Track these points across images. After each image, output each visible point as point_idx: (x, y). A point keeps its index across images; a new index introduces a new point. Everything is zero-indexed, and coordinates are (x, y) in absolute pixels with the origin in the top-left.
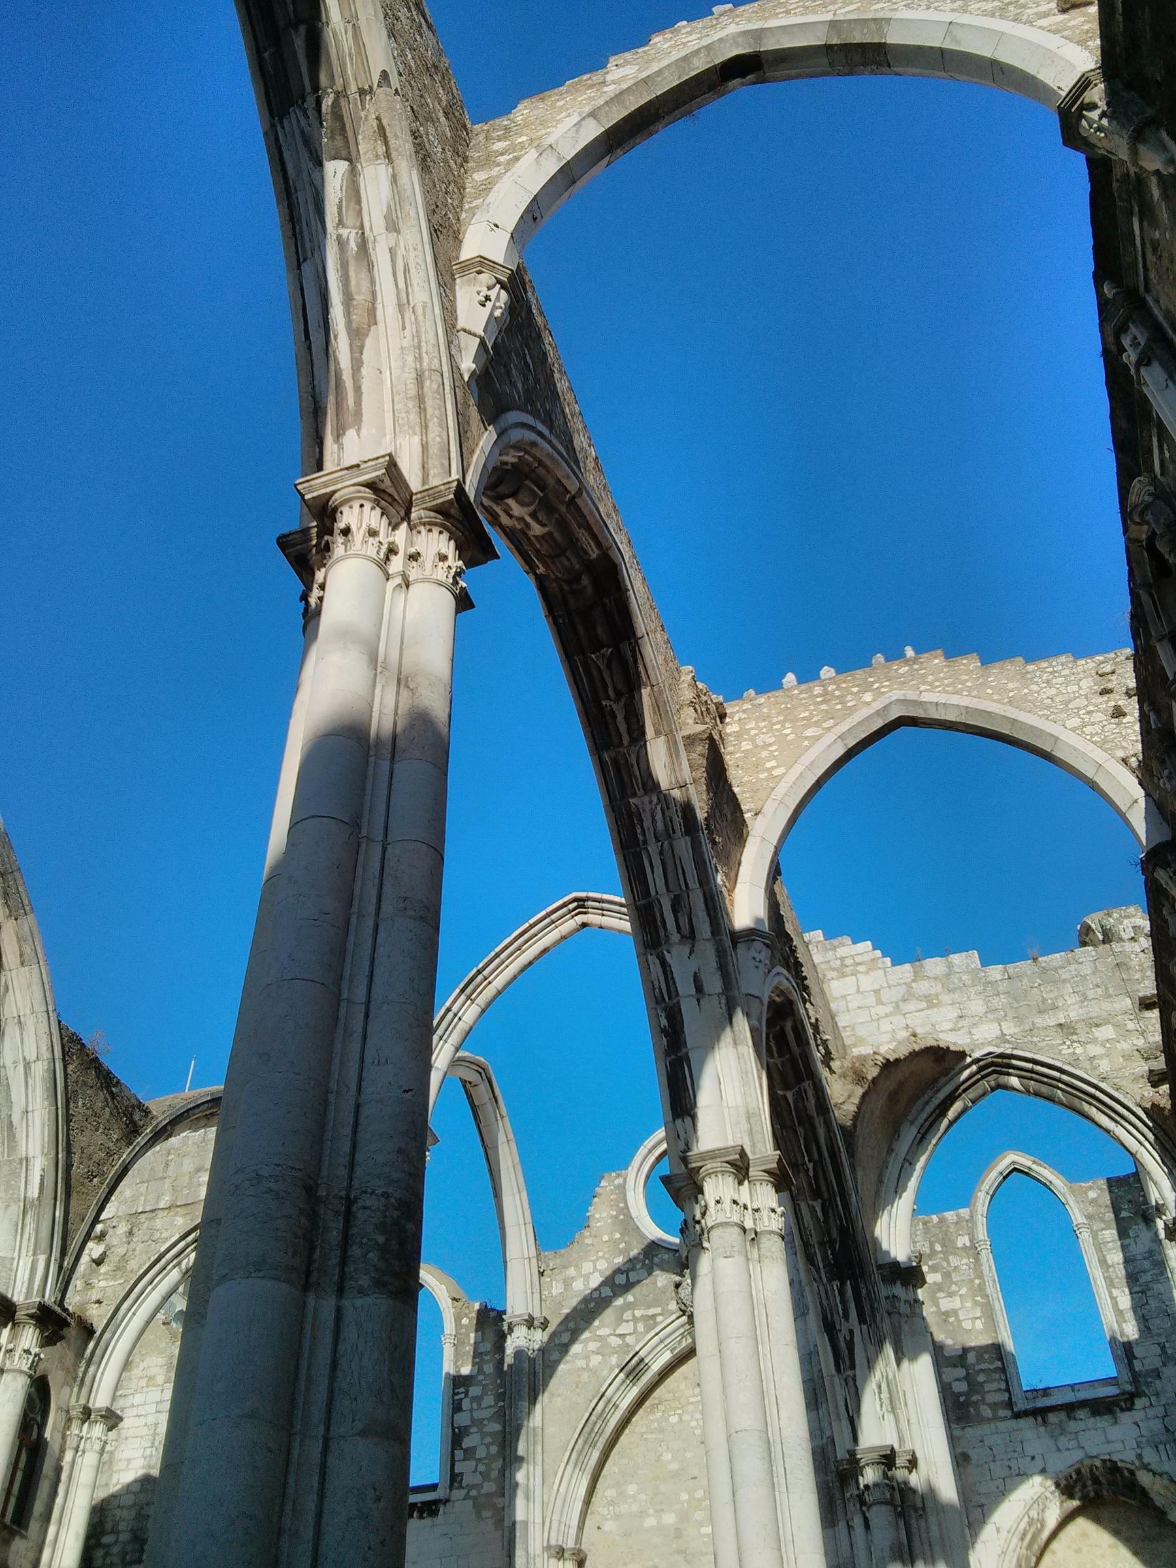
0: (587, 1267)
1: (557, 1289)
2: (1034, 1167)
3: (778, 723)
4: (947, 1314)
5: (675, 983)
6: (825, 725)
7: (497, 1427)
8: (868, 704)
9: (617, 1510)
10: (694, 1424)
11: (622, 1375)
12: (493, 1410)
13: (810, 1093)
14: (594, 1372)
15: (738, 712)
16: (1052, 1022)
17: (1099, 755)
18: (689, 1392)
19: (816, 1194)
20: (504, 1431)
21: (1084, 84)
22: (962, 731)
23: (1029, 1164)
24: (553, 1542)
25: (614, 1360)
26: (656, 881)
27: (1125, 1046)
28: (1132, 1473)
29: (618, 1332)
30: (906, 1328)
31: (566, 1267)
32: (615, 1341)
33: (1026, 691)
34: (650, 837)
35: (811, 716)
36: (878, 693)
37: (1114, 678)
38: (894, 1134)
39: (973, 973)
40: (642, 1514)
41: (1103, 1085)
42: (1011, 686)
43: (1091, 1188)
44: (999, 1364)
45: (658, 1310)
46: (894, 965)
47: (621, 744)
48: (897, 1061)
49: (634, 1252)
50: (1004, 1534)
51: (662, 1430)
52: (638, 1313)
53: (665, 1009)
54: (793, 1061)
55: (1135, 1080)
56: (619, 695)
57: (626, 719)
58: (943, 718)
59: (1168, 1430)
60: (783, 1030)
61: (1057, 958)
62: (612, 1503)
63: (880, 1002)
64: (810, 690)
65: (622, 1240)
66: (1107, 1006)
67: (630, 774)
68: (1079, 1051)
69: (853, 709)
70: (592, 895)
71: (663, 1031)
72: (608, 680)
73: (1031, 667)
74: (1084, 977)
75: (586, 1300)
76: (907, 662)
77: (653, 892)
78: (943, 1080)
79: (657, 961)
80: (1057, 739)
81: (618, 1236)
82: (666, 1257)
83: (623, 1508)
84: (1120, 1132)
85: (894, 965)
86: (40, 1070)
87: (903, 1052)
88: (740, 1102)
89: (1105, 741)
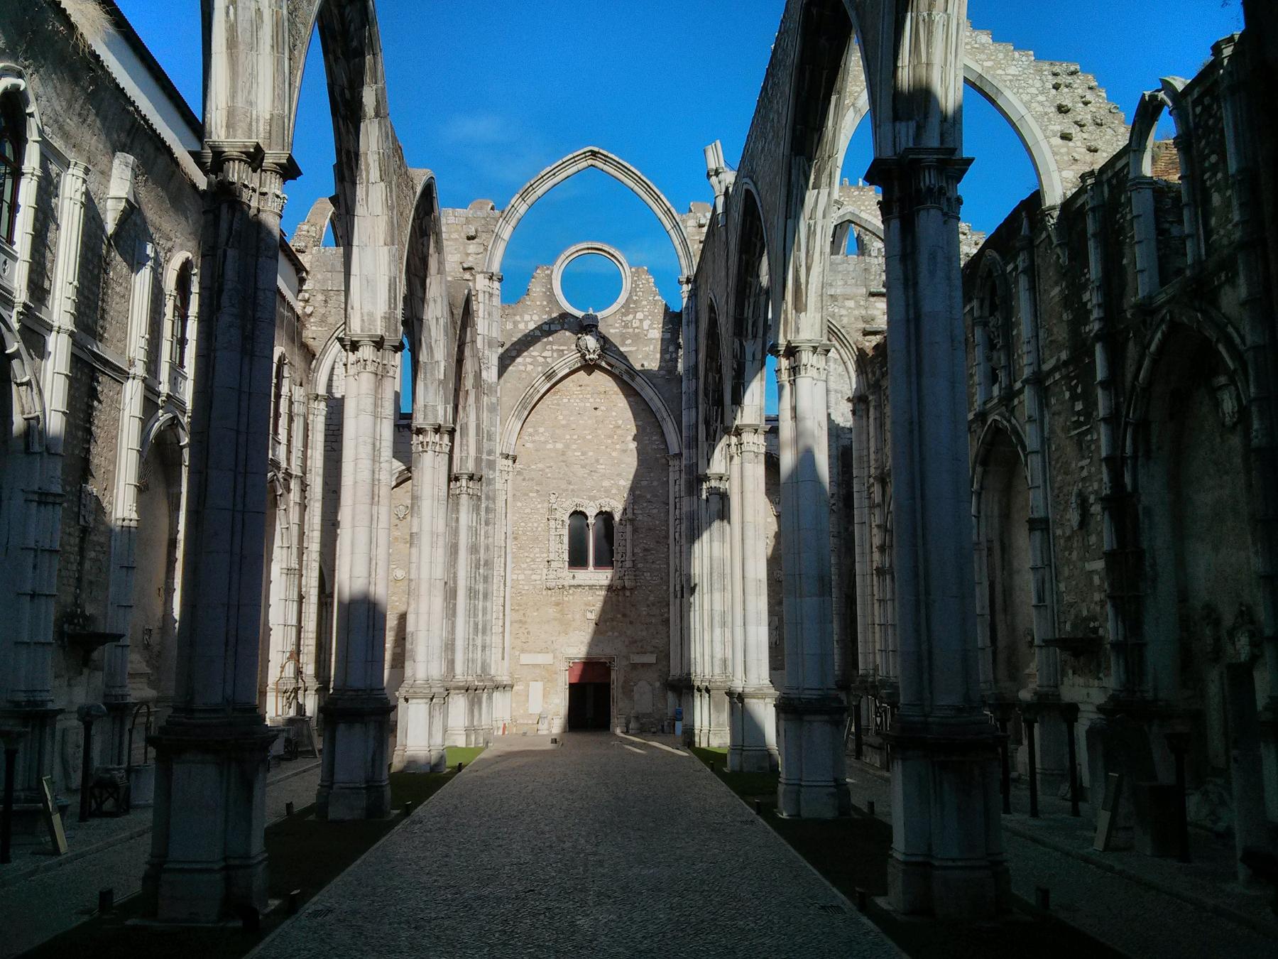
0: (527, 317)
1: (509, 326)
14: (528, 373)
21: (1053, 208)
25: (540, 369)
26: (748, 313)
27: (856, 312)
40: (546, 442)
49: (554, 315)
51: (558, 405)
62: (530, 435)
66: (854, 290)
75: (526, 336)
76: (858, 188)
83: (537, 438)
84: (842, 351)
86: (442, 322)
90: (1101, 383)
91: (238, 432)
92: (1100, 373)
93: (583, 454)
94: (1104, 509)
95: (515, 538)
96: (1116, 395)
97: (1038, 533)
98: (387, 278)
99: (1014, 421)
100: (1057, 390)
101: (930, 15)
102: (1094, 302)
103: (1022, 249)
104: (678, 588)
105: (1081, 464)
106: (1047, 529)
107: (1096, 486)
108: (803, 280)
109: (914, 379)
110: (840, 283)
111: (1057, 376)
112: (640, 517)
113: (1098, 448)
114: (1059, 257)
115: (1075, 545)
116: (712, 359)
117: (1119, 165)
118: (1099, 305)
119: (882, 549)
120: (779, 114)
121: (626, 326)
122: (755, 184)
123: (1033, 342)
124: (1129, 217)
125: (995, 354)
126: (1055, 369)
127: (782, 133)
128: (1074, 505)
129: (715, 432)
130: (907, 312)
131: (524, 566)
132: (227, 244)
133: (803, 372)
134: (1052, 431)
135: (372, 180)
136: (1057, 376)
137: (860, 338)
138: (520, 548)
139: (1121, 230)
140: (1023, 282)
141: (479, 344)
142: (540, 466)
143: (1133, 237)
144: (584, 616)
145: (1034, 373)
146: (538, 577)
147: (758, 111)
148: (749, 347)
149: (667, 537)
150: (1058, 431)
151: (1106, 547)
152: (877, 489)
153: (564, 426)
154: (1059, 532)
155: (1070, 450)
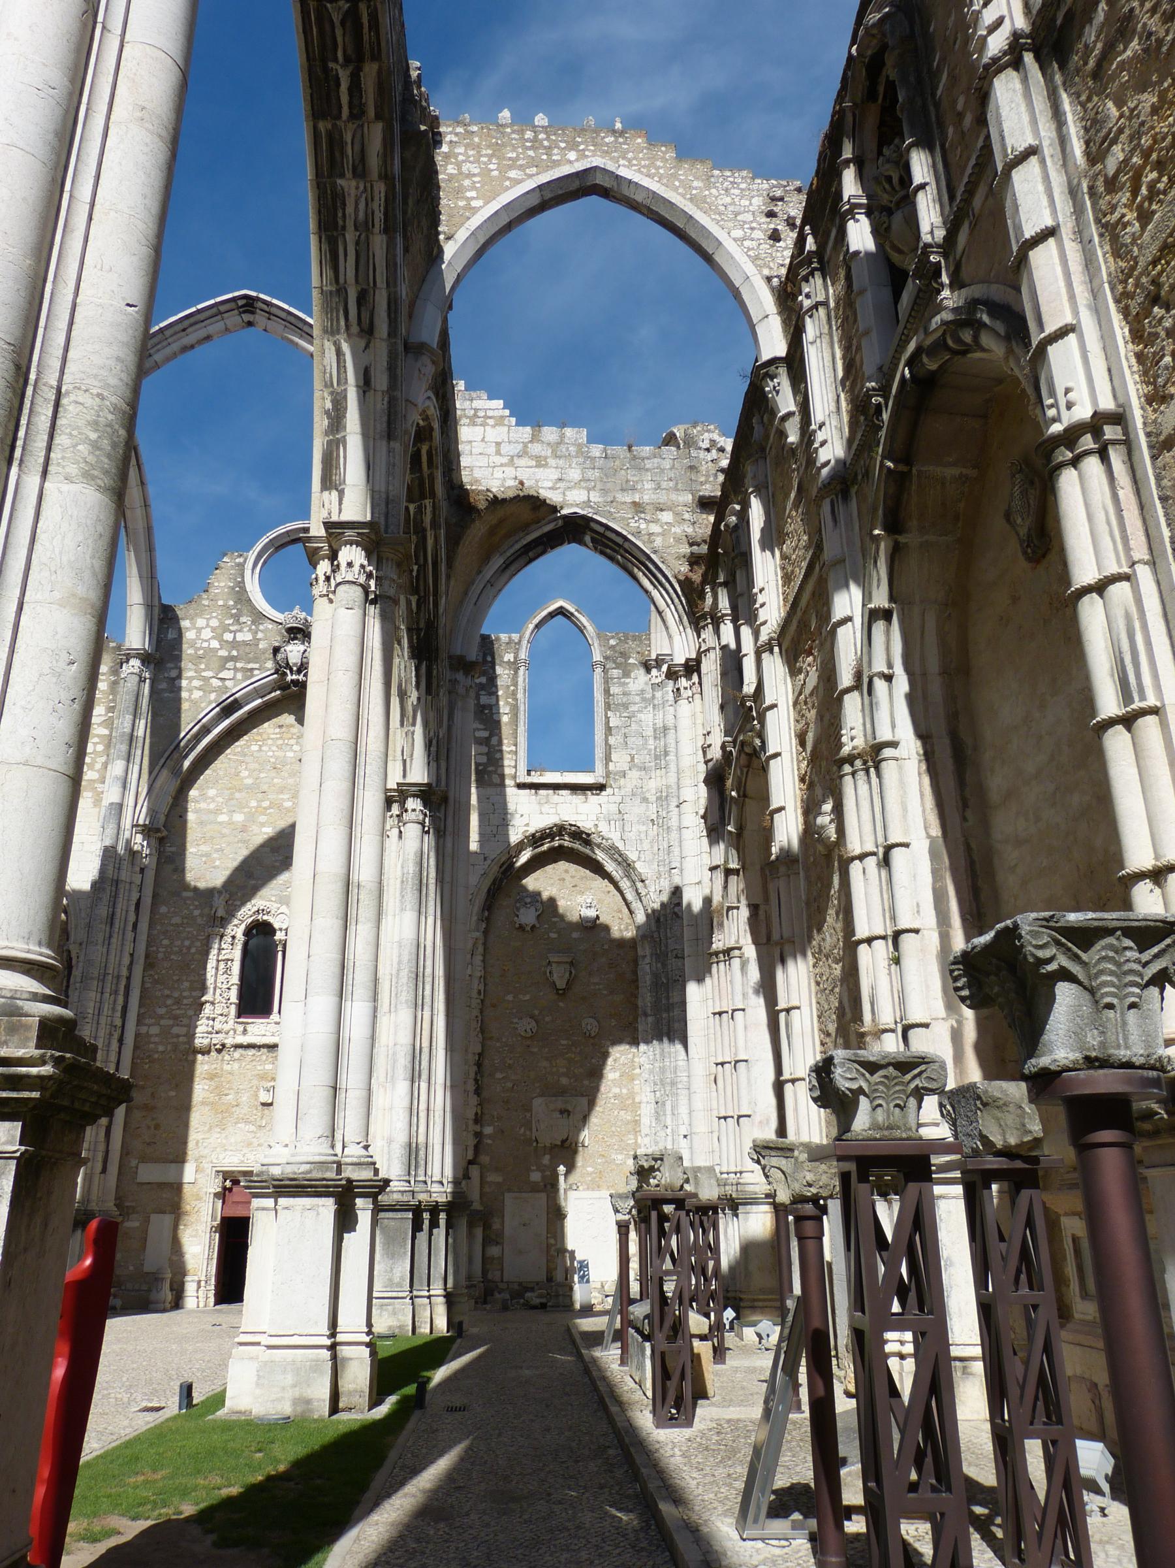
0: (201, 622)
2: (576, 614)
3: (486, 155)
4: (484, 707)
5: (345, 372)
6: (528, 171)
7: (106, 732)
8: (571, 162)
9: (198, 806)
10: (270, 754)
11: (218, 709)
12: (104, 718)
13: (429, 510)
15: (451, 133)
16: (628, 499)
17: (749, 268)
18: (271, 731)
19: (415, 590)
20: (111, 735)
22: (643, 214)
23: (572, 610)
25: (213, 696)
27: (677, 530)
28: (588, 835)
29: (220, 676)
30: (460, 704)
32: (215, 683)
33: (707, 193)
35: (517, 158)
36: (582, 156)
37: (780, 203)
38: (486, 559)
39: (580, 446)
40: (218, 811)
41: (653, 556)
42: (695, 184)
43: (613, 637)
44: (513, 748)
45: (257, 666)
46: (517, 424)
47: (339, 117)
48: (504, 500)
50: (489, 862)
52: (239, 665)
53: (332, 393)
54: (421, 481)
55: (678, 558)
56: (347, 60)
57: (350, 89)
58: (632, 196)
59: (620, 812)
60: (418, 452)
61: (647, 450)
63: (498, 453)
64: (522, 132)
65: (234, 607)
68: (643, 526)
69: (556, 164)
70: (262, 296)
71: (327, 412)
72: (340, 39)
73: (716, 172)
74: (663, 470)
78: (534, 526)
79: (333, 348)
80: (720, 243)
81: (231, 603)
82: (270, 626)
83: (203, 805)
84: (655, 594)
85: (517, 424)
87: (510, 494)
88: (383, 489)
89: (757, 258)
95: (150, 964)
110: (648, 486)
131: (162, 1011)
137: (684, 568)
138: (156, 982)
142: (204, 848)
144: (256, 1096)
146: (183, 1030)
153: (249, 788)
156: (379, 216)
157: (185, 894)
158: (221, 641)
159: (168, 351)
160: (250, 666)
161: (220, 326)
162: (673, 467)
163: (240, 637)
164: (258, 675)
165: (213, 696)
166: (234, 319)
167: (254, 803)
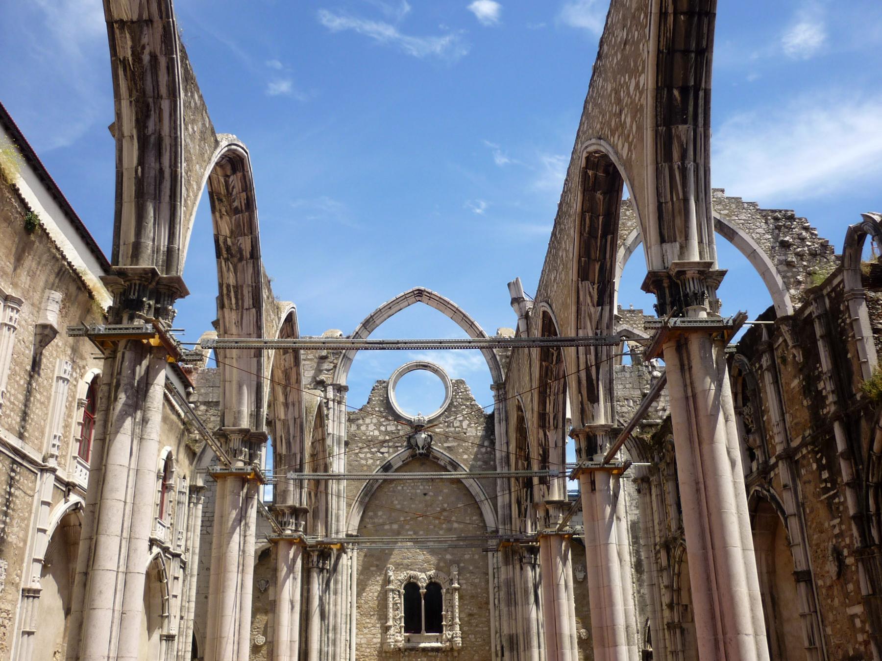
0: (368, 421)
14: (369, 466)
21: (787, 318)
24: (350, 532)
25: (378, 462)
26: (549, 408)
29: (382, 450)
31: (358, 419)
32: (379, 455)
34: (552, 394)
40: (384, 524)
51: (394, 491)
52: (390, 444)
62: (371, 518)
67: (552, 373)
77: (547, 411)
83: (376, 520)
90: (842, 454)
91: (125, 502)
92: (841, 445)
93: (415, 533)
94: (857, 561)
95: (358, 607)
96: (856, 465)
97: (802, 585)
98: (255, 383)
99: (772, 491)
100: (805, 462)
101: (683, 164)
102: (828, 388)
103: (764, 352)
104: (499, 648)
105: (832, 523)
106: (811, 581)
107: (848, 541)
108: (594, 377)
109: (697, 445)
111: (804, 451)
112: (464, 587)
113: (846, 508)
114: (794, 356)
115: (836, 593)
116: (521, 449)
117: (836, 282)
118: (833, 392)
119: (671, 606)
120: (567, 251)
121: (448, 426)
122: (550, 306)
123: (781, 425)
124: (848, 321)
125: (751, 438)
126: (804, 444)
127: (570, 265)
128: (831, 558)
129: (526, 510)
130: (685, 391)
131: (366, 631)
132: (125, 348)
133: (599, 451)
134: (804, 497)
135: (246, 306)
136: (804, 451)
139: (843, 332)
140: (768, 377)
141: (329, 441)
143: (854, 336)
145: (784, 449)
147: (549, 252)
148: (552, 436)
149: (488, 603)
150: (810, 497)
151: (864, 592)
152: (663, 555)
154: (820, 583)
155: (823, 512)
156: (561, 388)
157: (372, 569)
158: (380, 431)
159: (382, 318)
160: (397, 444)
161: (406, 303)
162: (631, 376)
163: (389, 428)
164: (401, 450)
165: (378, 462)
166: (412, 299)
167: (402, 519)
